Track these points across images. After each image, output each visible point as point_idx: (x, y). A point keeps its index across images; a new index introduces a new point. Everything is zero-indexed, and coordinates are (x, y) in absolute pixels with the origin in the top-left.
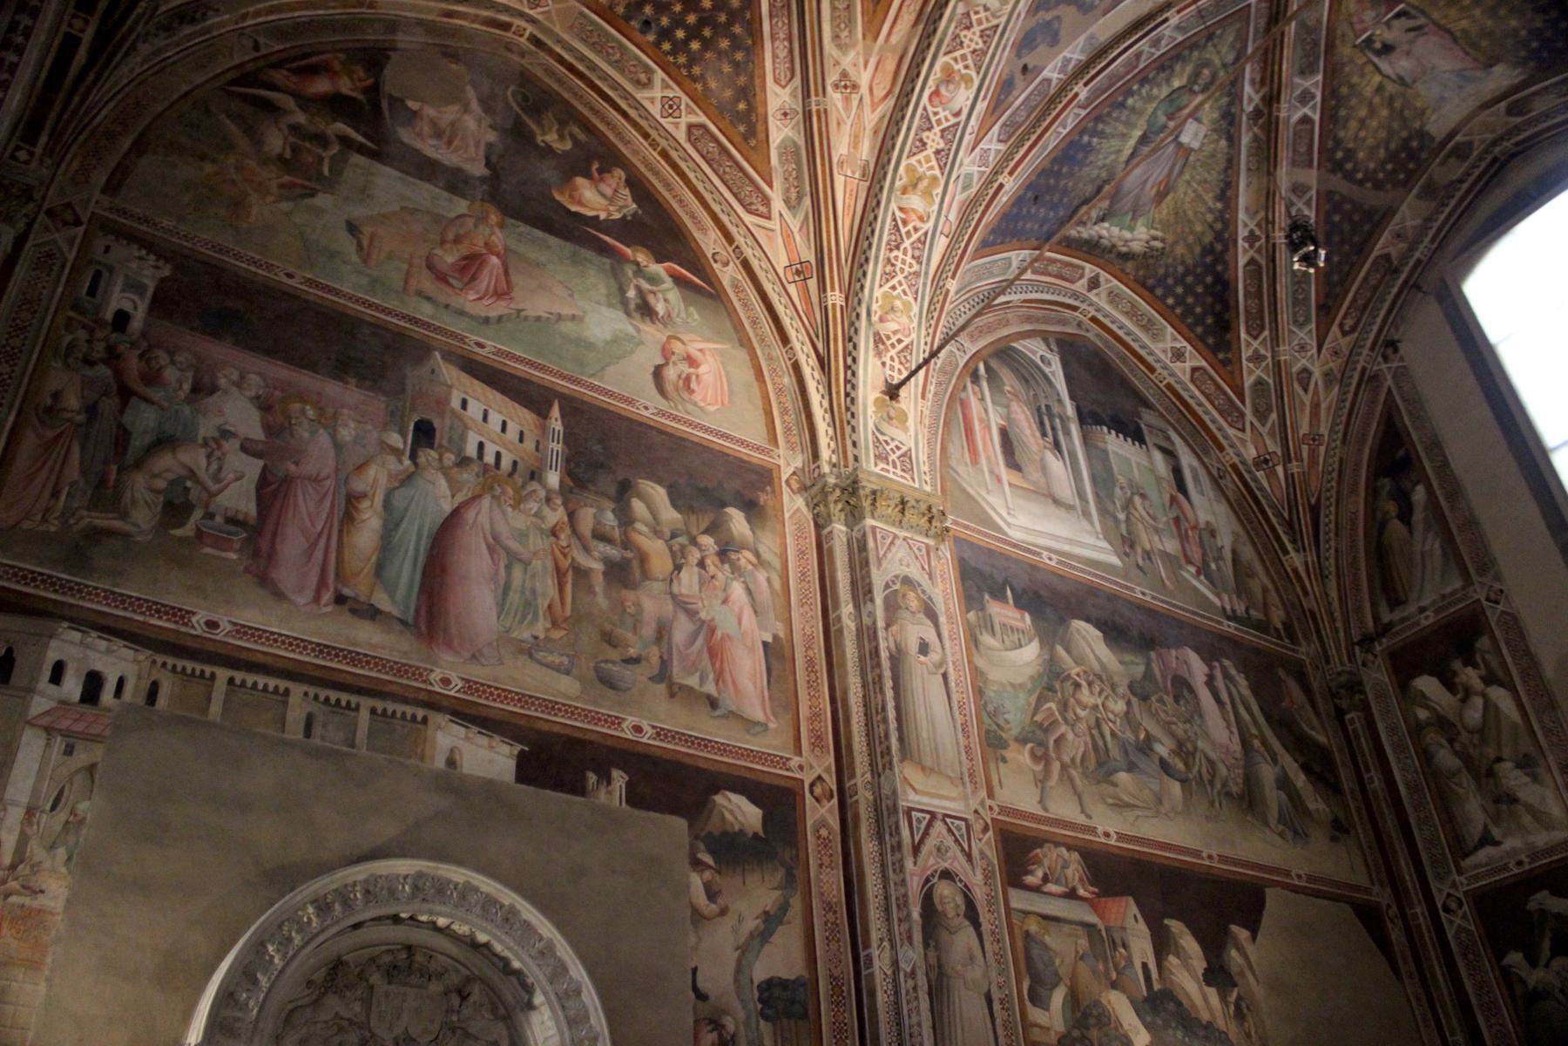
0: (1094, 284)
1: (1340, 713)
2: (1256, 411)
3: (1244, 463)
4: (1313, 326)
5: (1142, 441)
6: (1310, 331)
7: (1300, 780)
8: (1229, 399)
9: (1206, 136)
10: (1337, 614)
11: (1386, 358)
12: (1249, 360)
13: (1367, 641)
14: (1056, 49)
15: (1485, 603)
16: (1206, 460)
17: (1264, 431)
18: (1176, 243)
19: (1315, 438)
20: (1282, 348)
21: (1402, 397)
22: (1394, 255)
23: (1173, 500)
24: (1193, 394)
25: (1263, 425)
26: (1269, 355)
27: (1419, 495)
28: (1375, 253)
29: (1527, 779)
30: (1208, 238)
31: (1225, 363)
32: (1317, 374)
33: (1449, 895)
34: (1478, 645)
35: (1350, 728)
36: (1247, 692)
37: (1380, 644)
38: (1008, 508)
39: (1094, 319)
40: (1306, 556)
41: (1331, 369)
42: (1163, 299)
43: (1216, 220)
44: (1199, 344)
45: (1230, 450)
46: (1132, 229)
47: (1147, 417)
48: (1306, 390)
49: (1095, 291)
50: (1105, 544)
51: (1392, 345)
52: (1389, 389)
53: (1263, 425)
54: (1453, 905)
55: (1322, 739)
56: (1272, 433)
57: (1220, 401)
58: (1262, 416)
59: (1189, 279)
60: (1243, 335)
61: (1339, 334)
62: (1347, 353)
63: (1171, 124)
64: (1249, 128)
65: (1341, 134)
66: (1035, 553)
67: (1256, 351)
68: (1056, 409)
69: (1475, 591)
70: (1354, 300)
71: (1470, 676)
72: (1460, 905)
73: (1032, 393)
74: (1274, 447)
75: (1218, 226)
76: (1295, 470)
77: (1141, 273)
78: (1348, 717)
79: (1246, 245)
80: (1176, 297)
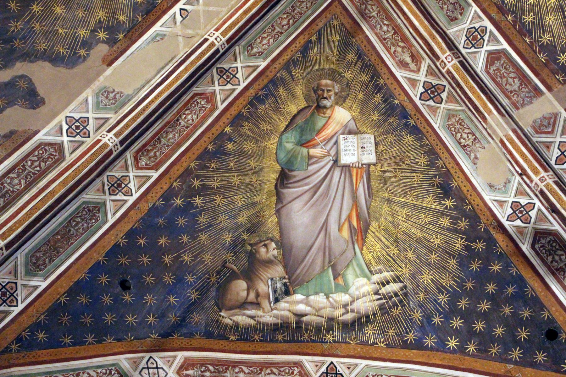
9: (377, 144)
14: (43, 110)
18: (413, 276)
30: (459, 244)
42: (441, 347)
43: (455, 220)
46: (345, 289)
59: (463, 303)
63: (314, 152)
64: (434, 110)
65: (546, 38)
75: (463, 224)
77: (391, 332)
79: (518, 223)
80: (456, 332)
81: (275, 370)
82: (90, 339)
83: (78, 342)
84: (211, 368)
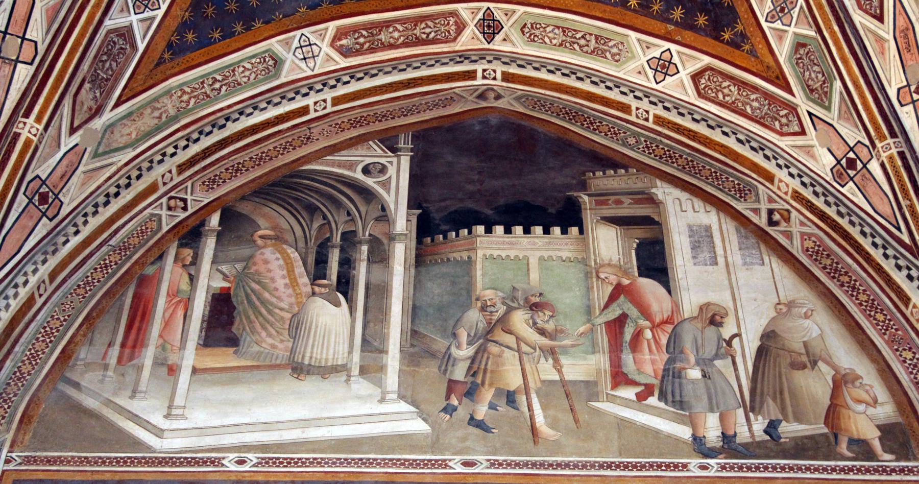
0: (490, 27)
2: (810, 90)
8: (767, 95)
12: (770, 18)
16: (739, 206)
17: (832, 116)
25: (828, 109)
38: (170, 407)
39: (507, 77)
44: (689, 36)
45: (782, 174)
48: (880, 18)
49: (499, 37)
50: (404, 407)
53: (828, 109)
57: (754, 103)
58: (820, 95)
66: (204, 462)
68: (366, 230)
73: (316, 225)
81: (430, 23)
82: (239, 28)
83: (228, 34)
84: (364, 33)
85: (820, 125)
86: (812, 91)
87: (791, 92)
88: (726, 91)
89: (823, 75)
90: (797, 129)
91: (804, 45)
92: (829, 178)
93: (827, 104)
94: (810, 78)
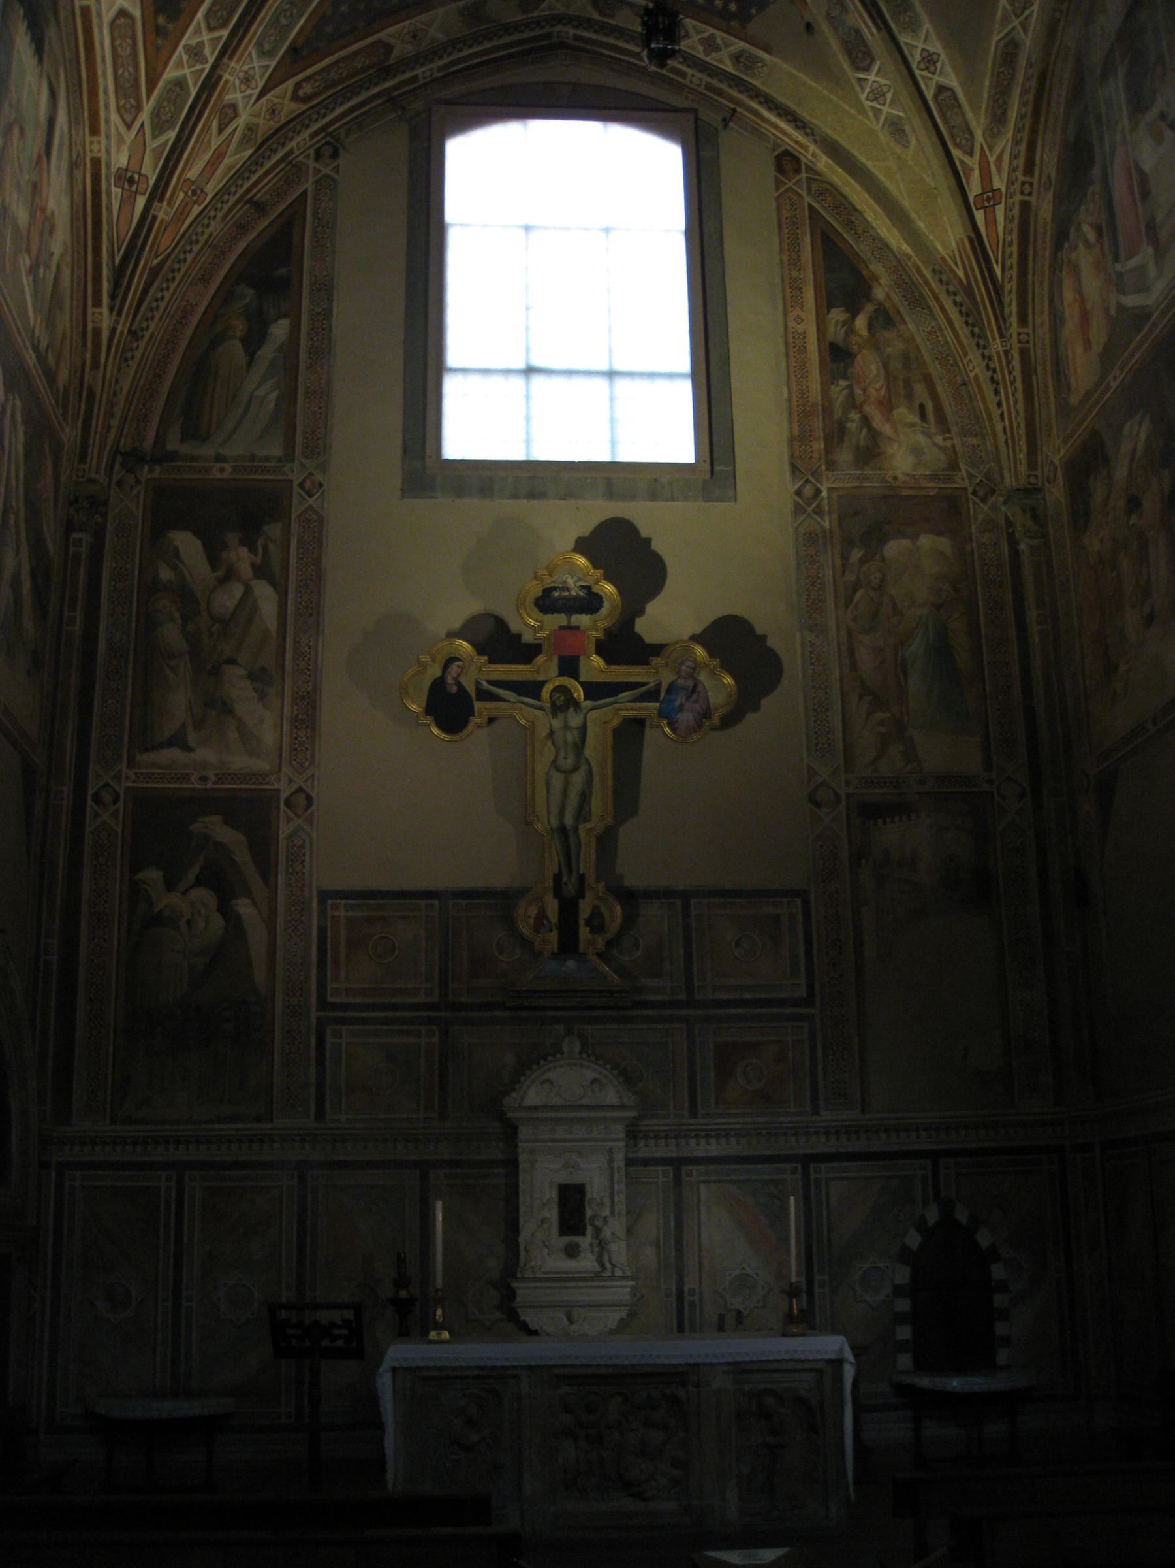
1: (69, 527)
2: (156, 114)
3: (108, 165)
4: (273, 64)
5: (41, 61)
6: (267, 67)
7: (26, 587)
8: (137, 79)
10: (118, 411)
11: (318, 156)
12: (188, 48)
13: (133, 458)
15: (296, 489)
17: (151, 144)
19: (197, 192)
20: (233, 64)
21: (315, 214)
22: (396, 52)
23: (39, 158)
24: (104, 39)
25: (154, 137)
26: (211, 61)
27: (280, 330)
28: (381, 35)
29: (254, 694)
31: (160, 31)
32: (242, 121)
33: (107, 785)
34: (266, 528)
35: (72, 550)
36: (21, 450)
37: (151, 471)
40: (117, 322)
41: (258, 126)
45: (103, 139)
47: (51, 35)
48: (221, 130)
51: (331, 149)
52: (305, 192)
53: (154, 137)
54: (107, 798)
55: (51, 548)
56: (157, 153)
58: (159, 126)
60: (200, 15)
61: (289, 95)
62: (283, 121)
67: (201, 45)
69: (293, 471)
70: (326, 69)
71: (242, 558)
72: (116, 800)
74: (150, 171)
76: (161, 215)
78: (75, 535)
85: (140, 137)
86: (158, 115)
87: (148, 98)
88: (124, 44)
89: (172, 117)
90: (129, 120)
91: (182, 88)
92: (113, 170)
93: (156, 133)
94: (165, 108)
